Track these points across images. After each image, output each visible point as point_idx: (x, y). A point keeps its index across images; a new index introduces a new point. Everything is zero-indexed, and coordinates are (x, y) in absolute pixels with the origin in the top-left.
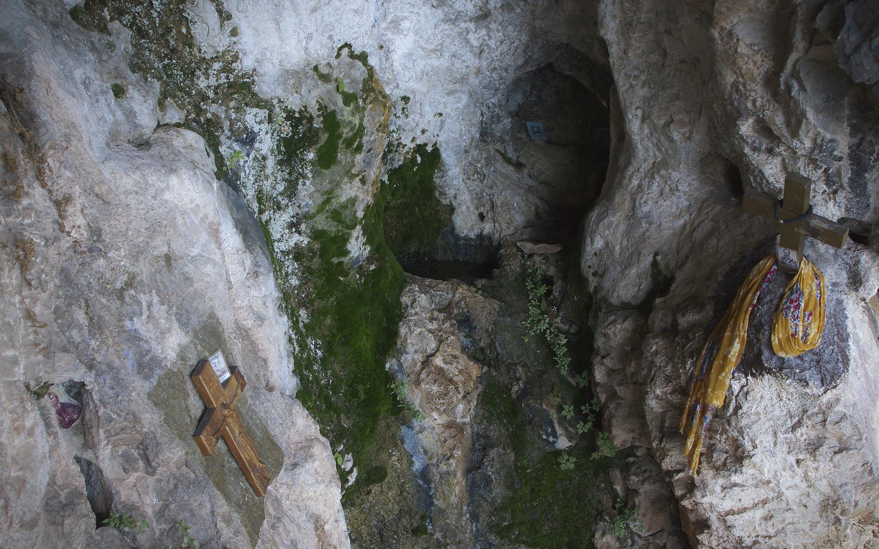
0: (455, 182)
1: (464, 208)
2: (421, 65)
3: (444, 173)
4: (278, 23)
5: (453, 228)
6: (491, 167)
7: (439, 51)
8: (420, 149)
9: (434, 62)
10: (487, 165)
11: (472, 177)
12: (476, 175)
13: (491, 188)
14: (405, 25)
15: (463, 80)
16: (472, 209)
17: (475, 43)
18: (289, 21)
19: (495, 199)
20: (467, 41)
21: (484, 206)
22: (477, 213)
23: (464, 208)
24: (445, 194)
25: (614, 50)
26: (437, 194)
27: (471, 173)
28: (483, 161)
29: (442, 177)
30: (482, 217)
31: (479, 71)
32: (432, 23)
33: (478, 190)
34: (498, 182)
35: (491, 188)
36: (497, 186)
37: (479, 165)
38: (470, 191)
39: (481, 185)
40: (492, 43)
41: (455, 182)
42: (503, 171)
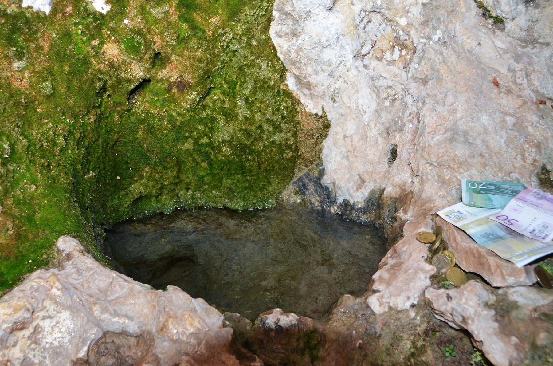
1: (351, 127)
5: (322, 173)
6: (435, 29)
10: (425, 23)
11: (387, 56)
12: (397, 52)
13: (425, 82)
16: (373, 132)
19: (425, 111)
21: (401, 130)
22: (384, 147)
23: (351, 127)
24: (308, 85)
26: (291, 83)
27: (385, 44)
28: (416, 11)
29: (294, 34)
30: (394, 154)
33: (399, 89)
34: (443, 70)
35: (425, 82)
36: (439, 80)
37: (403, 22)
38: (377, 90)
39: (404, 75)
41: (329, 55)
42: (471, 43)
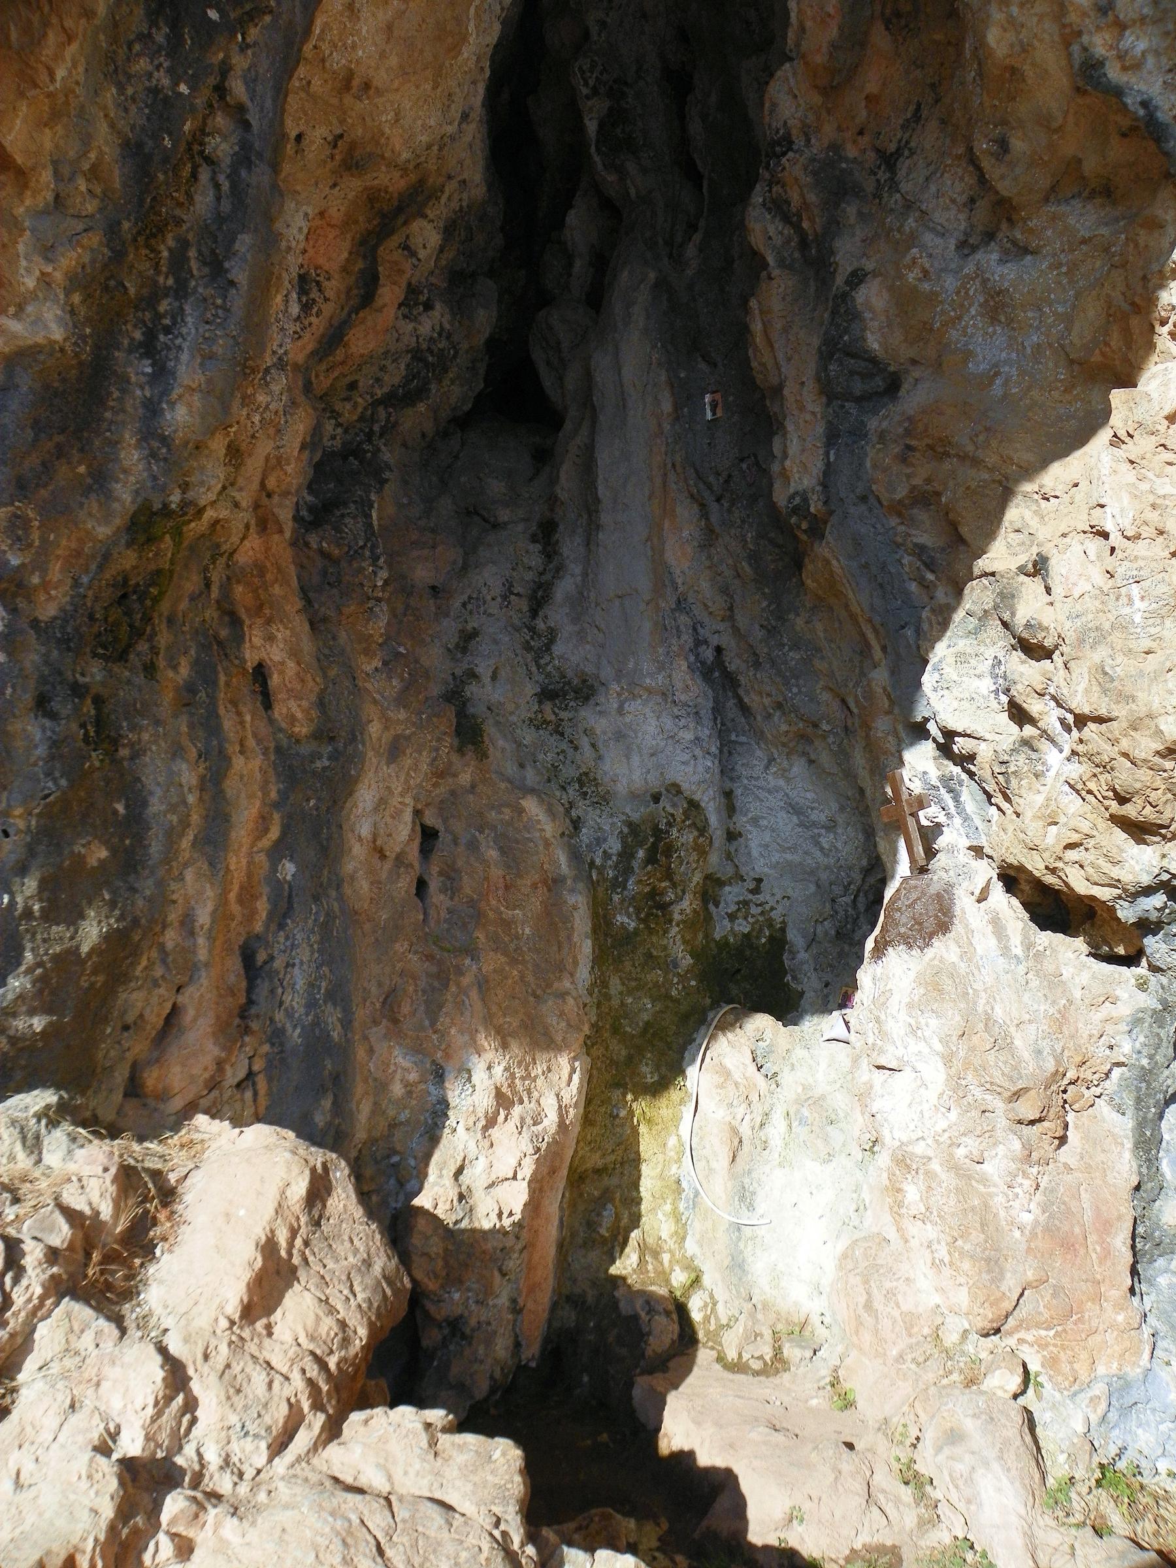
0: (805, 967)
2: (776, 857)
3: (793, 954)
4: (628, 757)
7: (793, 849)
8: (770, 923)
9: (789, 857)
14: (765, 823)
15: (812, 872)
17: (826, 846)
18: (636, 760)
20: (818, 844)
25: (868, 793)
31: (827, 867)
32: (790, 826)
40: (839, 845)
